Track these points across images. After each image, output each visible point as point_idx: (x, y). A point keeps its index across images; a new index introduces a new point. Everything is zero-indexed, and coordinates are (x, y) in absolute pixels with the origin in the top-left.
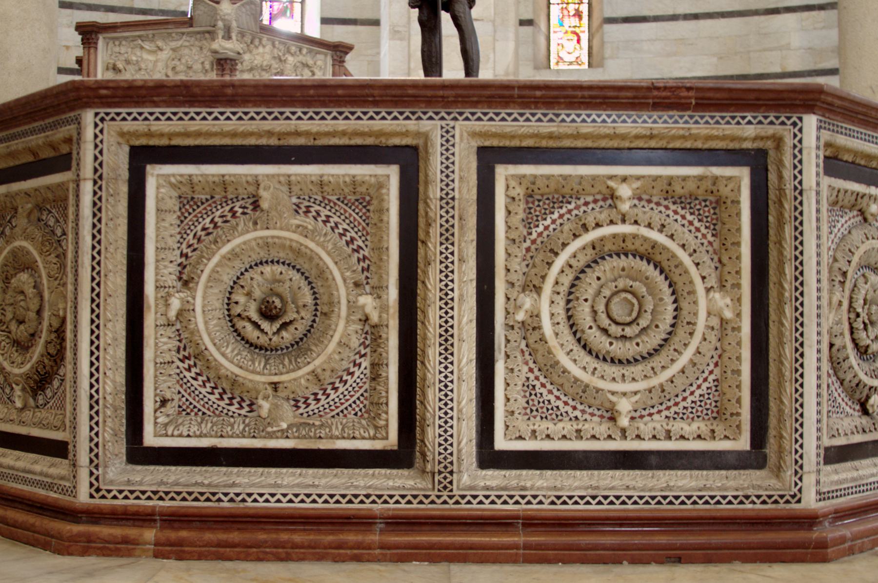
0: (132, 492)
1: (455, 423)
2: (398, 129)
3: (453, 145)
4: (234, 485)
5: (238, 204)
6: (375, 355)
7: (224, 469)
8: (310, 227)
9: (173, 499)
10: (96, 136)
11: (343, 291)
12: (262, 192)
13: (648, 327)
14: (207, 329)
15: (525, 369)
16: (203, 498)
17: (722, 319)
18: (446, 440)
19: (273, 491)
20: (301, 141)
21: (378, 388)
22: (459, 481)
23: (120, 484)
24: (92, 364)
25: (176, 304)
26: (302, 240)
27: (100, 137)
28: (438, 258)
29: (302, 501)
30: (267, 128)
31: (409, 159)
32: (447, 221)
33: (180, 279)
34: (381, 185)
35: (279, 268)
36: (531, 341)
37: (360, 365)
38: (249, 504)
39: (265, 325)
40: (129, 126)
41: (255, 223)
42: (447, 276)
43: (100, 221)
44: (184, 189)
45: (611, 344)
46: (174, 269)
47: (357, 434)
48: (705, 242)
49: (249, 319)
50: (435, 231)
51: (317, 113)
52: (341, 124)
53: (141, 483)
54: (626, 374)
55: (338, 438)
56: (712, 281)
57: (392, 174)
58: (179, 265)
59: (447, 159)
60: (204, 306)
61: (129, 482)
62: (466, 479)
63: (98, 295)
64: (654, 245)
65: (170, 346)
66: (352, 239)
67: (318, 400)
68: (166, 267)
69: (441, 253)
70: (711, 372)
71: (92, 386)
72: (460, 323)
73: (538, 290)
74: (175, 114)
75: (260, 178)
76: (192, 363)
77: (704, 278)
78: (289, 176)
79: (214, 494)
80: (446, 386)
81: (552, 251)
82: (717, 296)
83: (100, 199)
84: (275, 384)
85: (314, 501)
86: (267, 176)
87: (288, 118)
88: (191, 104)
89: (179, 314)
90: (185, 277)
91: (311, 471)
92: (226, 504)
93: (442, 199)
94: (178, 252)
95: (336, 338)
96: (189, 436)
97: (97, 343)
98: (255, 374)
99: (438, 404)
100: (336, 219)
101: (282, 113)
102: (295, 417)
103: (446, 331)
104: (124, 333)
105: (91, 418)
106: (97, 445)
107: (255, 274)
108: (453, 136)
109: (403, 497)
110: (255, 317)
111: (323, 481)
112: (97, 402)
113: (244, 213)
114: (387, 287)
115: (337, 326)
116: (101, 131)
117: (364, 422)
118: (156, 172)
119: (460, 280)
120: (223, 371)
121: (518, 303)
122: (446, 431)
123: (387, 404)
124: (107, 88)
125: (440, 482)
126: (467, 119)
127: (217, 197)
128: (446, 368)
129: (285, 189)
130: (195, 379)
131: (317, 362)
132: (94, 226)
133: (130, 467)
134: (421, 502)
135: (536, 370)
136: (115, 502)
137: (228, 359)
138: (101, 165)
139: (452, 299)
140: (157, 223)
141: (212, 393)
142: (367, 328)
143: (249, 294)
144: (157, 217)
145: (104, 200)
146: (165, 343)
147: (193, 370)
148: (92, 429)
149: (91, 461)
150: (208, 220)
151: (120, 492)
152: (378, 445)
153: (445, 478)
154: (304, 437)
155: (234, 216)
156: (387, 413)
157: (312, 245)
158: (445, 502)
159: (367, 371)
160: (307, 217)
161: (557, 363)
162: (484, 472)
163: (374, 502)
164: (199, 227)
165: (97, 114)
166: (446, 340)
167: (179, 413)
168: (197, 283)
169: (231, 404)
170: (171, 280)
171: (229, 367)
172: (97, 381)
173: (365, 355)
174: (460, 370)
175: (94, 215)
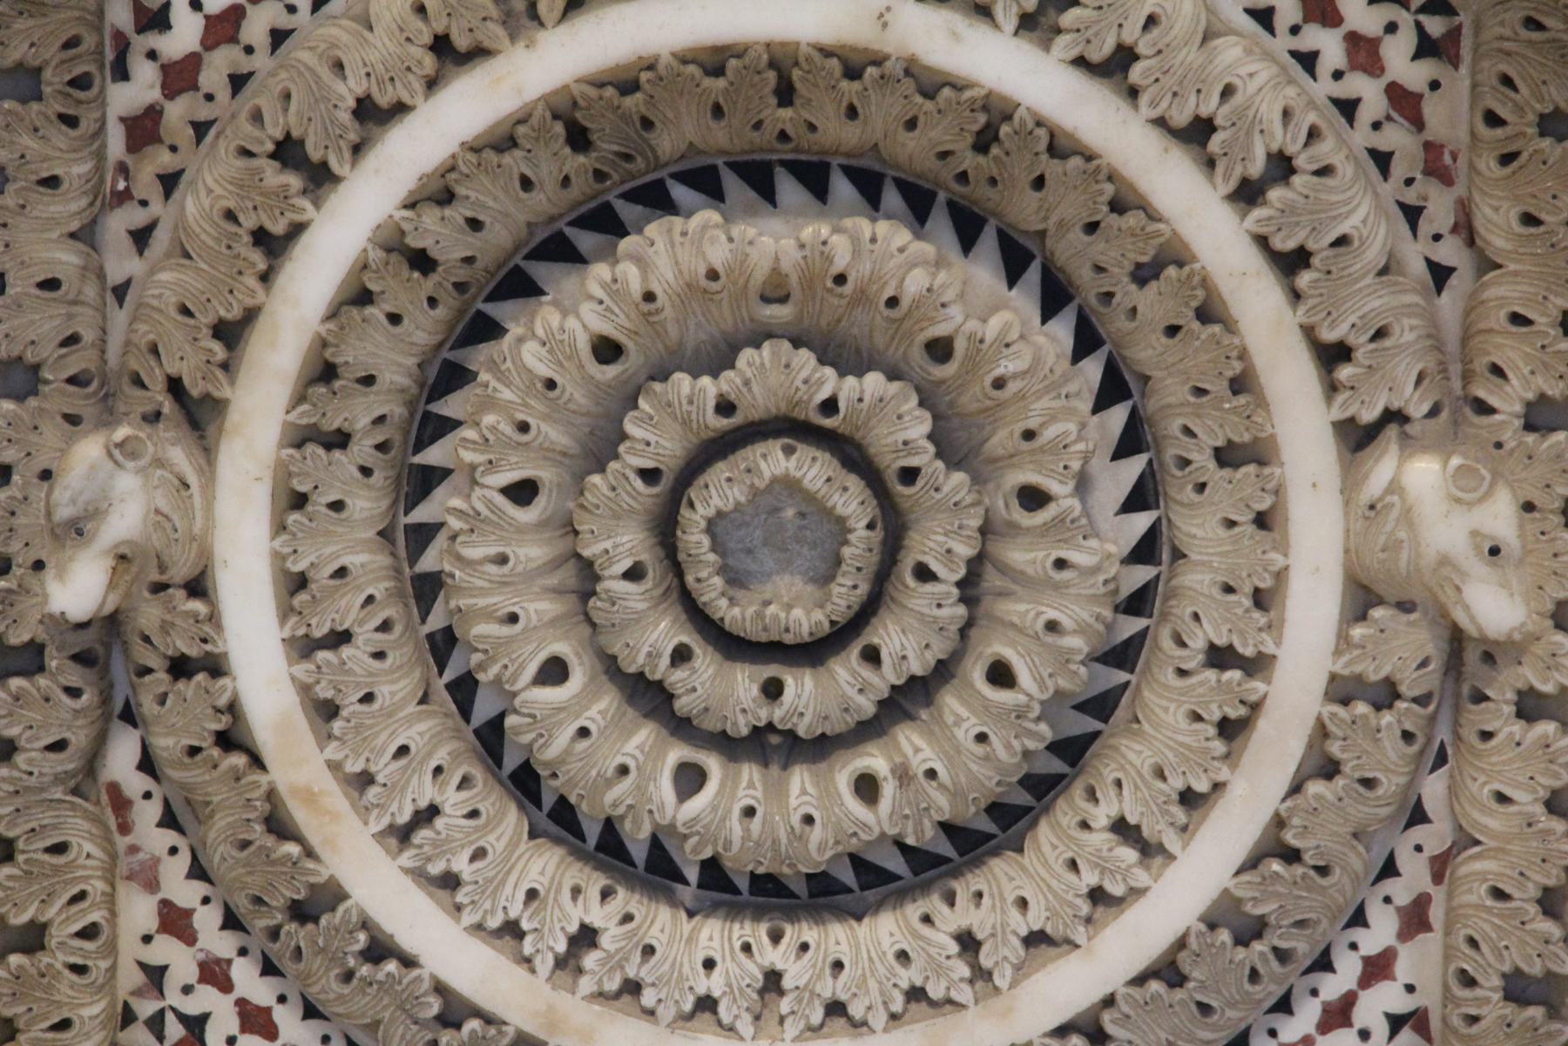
13: (944, 671)
15: (139, 912)
17: (1457, 639)
36: (167, 744)
45: (690, 779)
48: (1369, 92)
54: (795, 973)
56: (1394, 381)
64: (993, 121)
70: (1377, 968)
73: (198, 414)
77: (1332, 355)
81: (288, 151)
82: (1422, 475)
121: (65, 499)
135: (207, 921)
161: (333, 895)
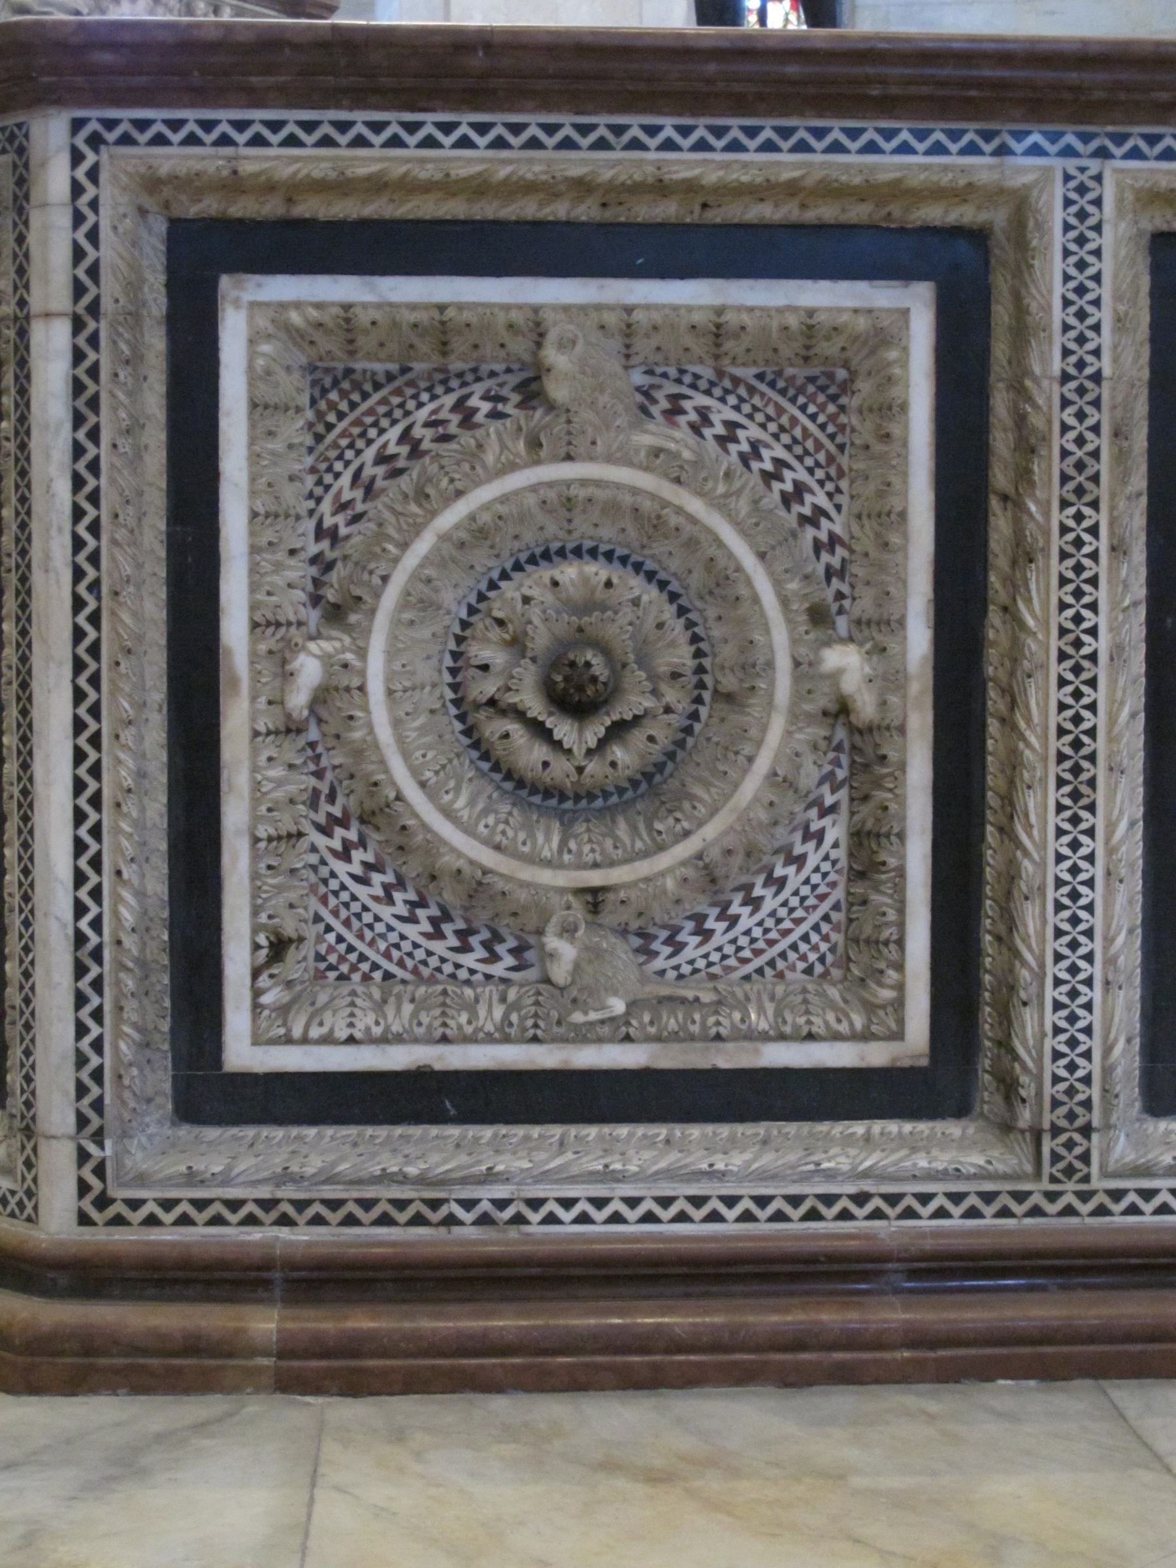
0: (201, 1204)
1: (1097, 994)
2: (946, 179)
3: (1098, 228)
4: (490, 1177)
5: (479, 389)
6: (865, 810)
7: (454, 1131)
8: (687, 454)
9: (318, 1220)
10: (77, 189)
11: (780, 636)
12: (552, 355)
14: (400, 740)
16: (402, 1217)
18: (1073, 1043)
19: (599, 1191)
20: (667, 210)
21: (875, 898)
22: (1106, 1151)
23: (167, 1182)
24: (79, 847)
25: (309, 670)
26: (669, 491)
27: (91, 191)
28: (1056, 543)
29: (682, 1217)
30: (575, 172)
31: (966, 270)
32: (1080, 441)
33: (316, 600)
34: (884, 336)
35: (598, 571)
37: (820, 836)
38: (535, 1228)
39: (564, 729)
40: (173, 159)
41: (535, 444)
42: (1078, 594)
43: (94, 435)
44: (326, 344)
46: (299, 571)
47: (818, 1027)
49: (519, 714)
50: (1049, 467)
51: (719, 132)
52: (787, 164)
53: (225, 1180)
55: (765, 1037)
57: (915, 310)
58: (314, 560)
59: (1081, 265)
60: (390, 676)
61: (192, 1178)
62: (1122, 1150)
63: (95, 650)
65: (292, 788)
66: (800, 489)
67: (707, 935)
68: (278, 567)
69: (1064, 530)
71: (80, 909)
72: (1112, 720)
74: (309, 126)
75: (548, 316)
76: (353, 835)
78: (629, 310)
79: (435, 1204)
80: (1075, 895)
83: (94, 372)
84: (595, 891)
85: (714, 1217)
86: (566, 308)
87: (635, 145)
88: (359, 99)
89: (321, 697)
90: (331, 595)
91: (695, 1131)
92: (469, 1232)
93: (1065, 378)
94: (310, 525)
95: (763, 763)
96: (351, 1040)
97: (93, 786)
98: (541, 865)
99: (1051, 945)
100: (755, 432)
101: (618, 130)
102: (644, 980)
103: (1077, 744)
104: (164, 757)
105: (80, 1000)
106: (98, 1075)
107: (534, 582)
108: (1098, 202)
109: (956, 1198)
110: (536, 707)
111: (737, 1161)
112: (97, 954)
113: (495, 415)
114: (902, 622)
115: (764, 729)
116: (93, 174)
117: (834, 993)
118: (247, 296)
119: (1114, 605)
120: (447, 860)
122: (1072, 1019)
123: (900, 943)
124: (114, 46)
125: (1056, 1158)
126: (1135, 154)
127: (419, 367)
128: (1075, 845)
129: (616, 344)
130: (363, 881)
131: (710, 831)
132: (78, 450)
133: (185, 1132)
134: (1005, 1213)
136: (155, 1235)
137: (459, 827)
138: (94, 272)
139: (1093, 657)
140: (252, 441)
141: (412, 919)
142: (841, 734)
143: (517, 644)
144: (253, 425)
145: (104, 375)
146: (279, 783)
147: (357, 855)
148: (81, 1030)
149: (82, 1121)
150: (394, 434)
151: (168, 1205)
152: (877, 1055)
153: (1070, 1145)
154: (674, 1037)
155: (468, 419)
156: (900, 967)
157: (695, 506)
158: (1069, 1211)
159: (840, 854)
160: (674, 424)
162: (1163, 1125)
163: (877, 1214)
164: (370, 454)
165: (77, 125)
166: (1076, 770)
167: (320, 976)
168: (373, 612)
169: (465, 948)
170: (293, 605)
171: (464, 847)
172: (96, 894)
173: (833, 809)
174: (1111, 851)
175: (78, 420)
